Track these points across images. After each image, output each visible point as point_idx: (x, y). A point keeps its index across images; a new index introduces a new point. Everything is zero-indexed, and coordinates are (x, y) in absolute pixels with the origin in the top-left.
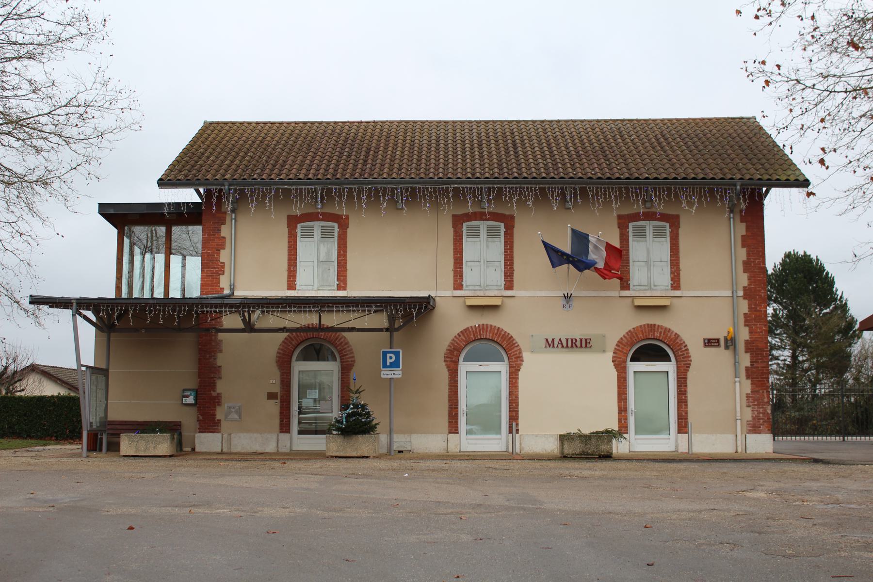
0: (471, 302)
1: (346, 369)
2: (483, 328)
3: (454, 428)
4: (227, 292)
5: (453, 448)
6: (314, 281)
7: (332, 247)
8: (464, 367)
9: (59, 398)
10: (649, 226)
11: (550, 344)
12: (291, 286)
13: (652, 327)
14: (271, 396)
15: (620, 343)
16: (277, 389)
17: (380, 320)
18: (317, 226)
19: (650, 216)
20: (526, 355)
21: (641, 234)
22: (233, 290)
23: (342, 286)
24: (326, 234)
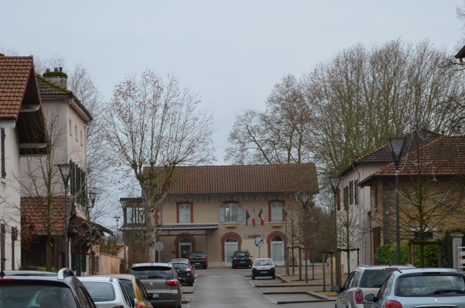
0: (227, 226)
1: (194, 244)
2: (231, 233)
3: (223, 260)
4: (160, 224)
5: (223, 265)
6: (184, 220)
7: (189, 211)
8: (226, 243)
9: (38, 266)
10: (277, 204)
11: (249, 237)
12: (178, 222)
13: (277, 232)
14: (173, 252)
15: (268, 236)
16: (175, 250)
17: (204, 232)
18: (185, 205)
19: (277, 201)
20: (243, 240)
21: (274, 206)
22: (162, 223)
23: (192, 222)
24: (187, 207)
